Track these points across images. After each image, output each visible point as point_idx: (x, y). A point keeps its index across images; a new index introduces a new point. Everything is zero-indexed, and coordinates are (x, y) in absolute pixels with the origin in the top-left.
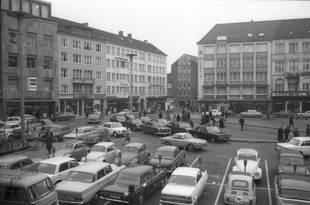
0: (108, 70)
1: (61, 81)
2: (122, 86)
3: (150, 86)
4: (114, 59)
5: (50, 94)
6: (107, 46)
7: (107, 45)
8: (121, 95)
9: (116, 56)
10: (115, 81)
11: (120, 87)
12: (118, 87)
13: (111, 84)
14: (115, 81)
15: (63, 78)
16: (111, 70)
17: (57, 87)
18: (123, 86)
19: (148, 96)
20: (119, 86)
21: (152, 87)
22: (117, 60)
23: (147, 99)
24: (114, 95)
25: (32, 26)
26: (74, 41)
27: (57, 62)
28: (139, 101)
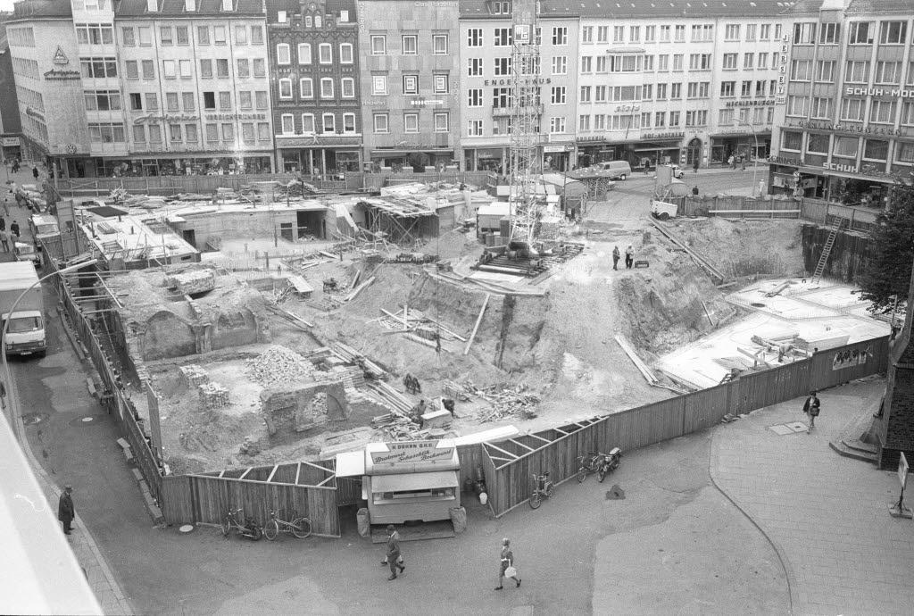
0: (585, 80)
1: (469, 113)
2: (620, 114)
3: (728, 105)
4: (605, 54)
5: (445, 136)
6: (585, 27)
7: (584, 23)
8: (616, 135)
9: (610, 47)
10: (606, 103)
11: (616, 117)
12: (609, 117)
13: (593, 109)
14: (606, 103)
15: (472, 106)
16: (594, 80)
17: (459, 125)
18: (626, 114)
19: (717, 131)
20: (613, 114)
21: (737, 110)
22: (612, 54)
23: (715, 139)
24: (599, 135)
25: (410, 17)
26: (497, 33)
27: (458, 77)
28: (684, 144)
